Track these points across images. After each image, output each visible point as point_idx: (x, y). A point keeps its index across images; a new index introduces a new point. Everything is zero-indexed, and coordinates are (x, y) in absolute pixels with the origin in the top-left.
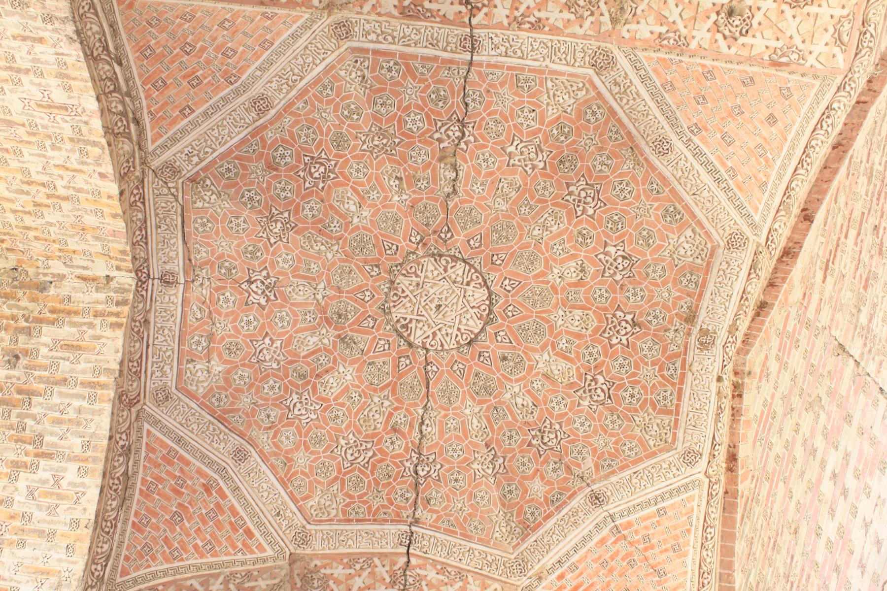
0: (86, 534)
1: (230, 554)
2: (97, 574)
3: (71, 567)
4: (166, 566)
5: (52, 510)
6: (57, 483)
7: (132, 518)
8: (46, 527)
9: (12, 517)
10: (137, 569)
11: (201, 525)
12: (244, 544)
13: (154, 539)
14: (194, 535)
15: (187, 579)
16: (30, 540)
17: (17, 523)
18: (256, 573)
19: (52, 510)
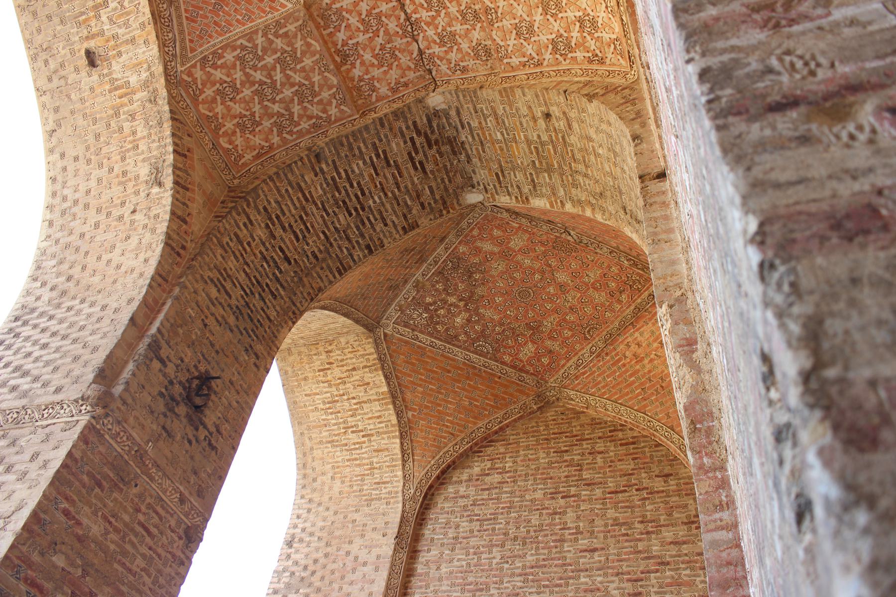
0: (150, 28)
1: (262, 17)
2: (170, 53)
3: (151, 53)
4: (221, 39)
5: (126, 25)
6: (122, 6)
7: (184, 14)
8: (128, 37)
9: (108, 41)
10: (201, 46)
11: (236, 6)
12: (271, 7)
13: (206, 25)
14: (234, 14)
15: (236, 40)
16: (123, 49)
17: (112, 43)
18: (282, 21)
19: (126, 25)
